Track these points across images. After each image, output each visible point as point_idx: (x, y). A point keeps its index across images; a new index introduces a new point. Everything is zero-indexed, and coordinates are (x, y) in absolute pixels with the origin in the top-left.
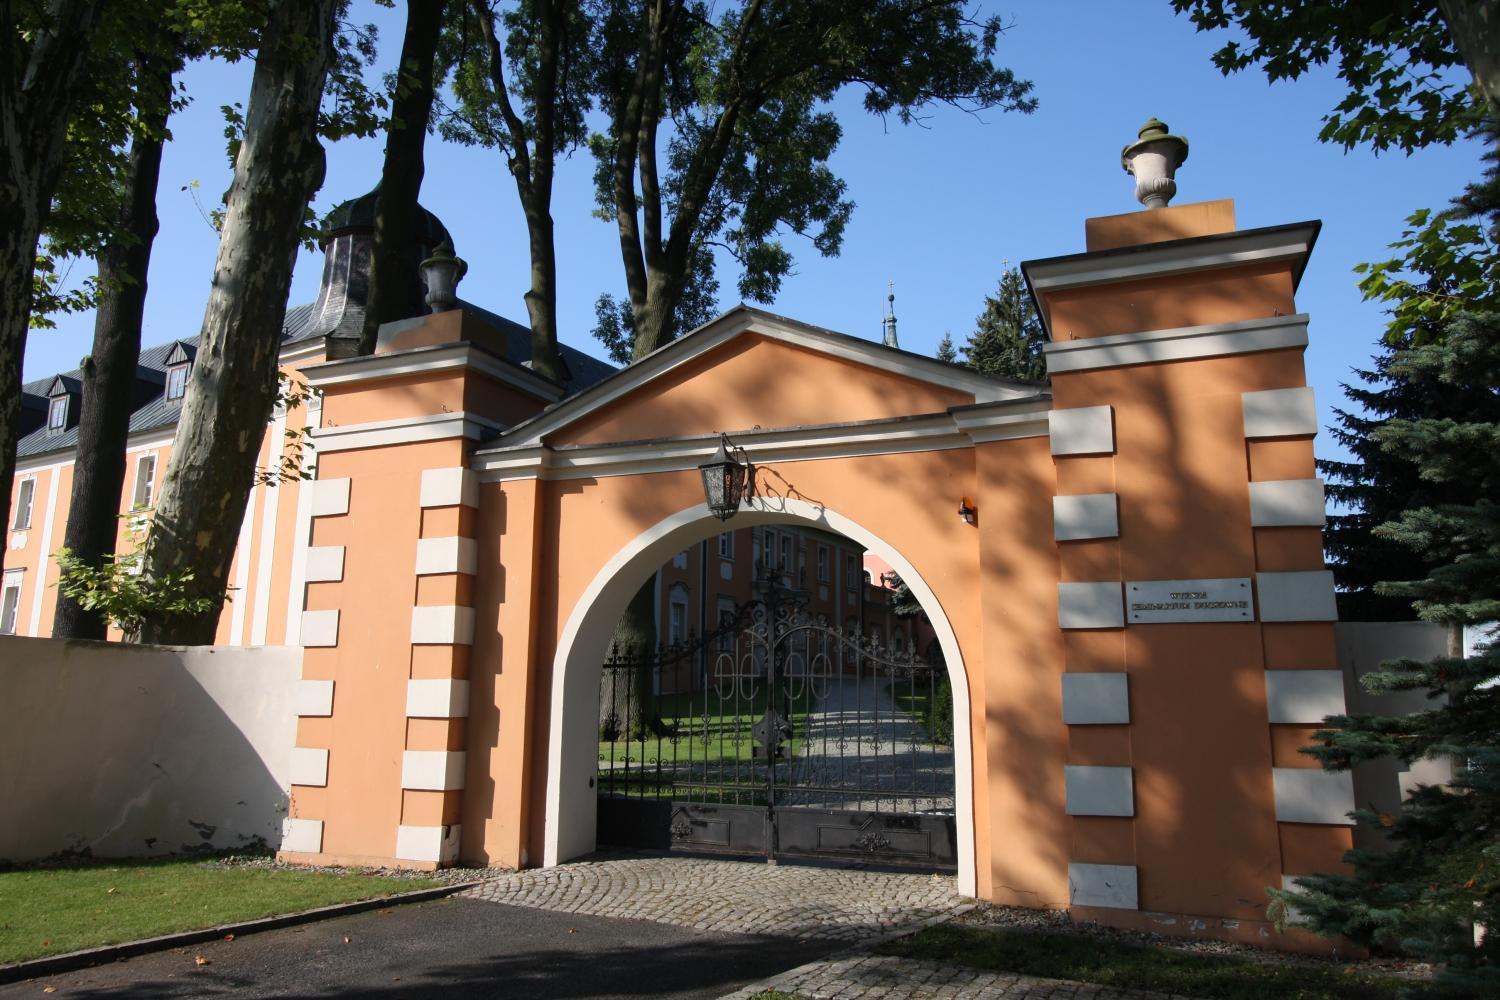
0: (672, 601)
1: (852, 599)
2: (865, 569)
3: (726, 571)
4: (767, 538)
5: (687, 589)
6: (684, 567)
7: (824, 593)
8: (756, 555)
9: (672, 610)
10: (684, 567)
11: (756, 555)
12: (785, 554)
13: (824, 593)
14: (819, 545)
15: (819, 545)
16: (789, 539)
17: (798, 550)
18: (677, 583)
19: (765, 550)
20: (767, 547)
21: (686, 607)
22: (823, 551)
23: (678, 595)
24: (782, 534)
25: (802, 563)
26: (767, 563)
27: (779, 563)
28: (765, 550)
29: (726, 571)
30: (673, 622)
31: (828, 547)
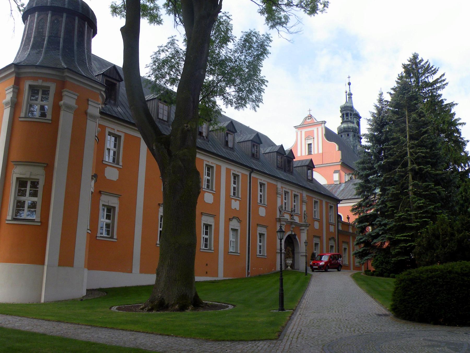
0: (231, 227)
1: (332, 229)
2: (339, 213)
3: (262, 212)
4: (285, 195)
5: (240, 221)
6: (238, 209)
7: (317, 225)
8: (279, 204)
9: (231, 233)
10: (238, 209)
11: (279, 204)
12: (295, 204)
13: (317, 225)
14: (314, 199)
15: (314, 199)
16: (297, 195)
17: (302, 201)
18: (234, 218)
19: (284, 201)
20: (285, 199)
21: (239, 231)
22: (316, 202)
23: (234, 224)
24: (294, 193)
25: (304, 208)
26: (285, 207)
27: (292, 209)
28: (284, 201)
29: (262, 212)
30: (232, 238)
31: (319, 201)
